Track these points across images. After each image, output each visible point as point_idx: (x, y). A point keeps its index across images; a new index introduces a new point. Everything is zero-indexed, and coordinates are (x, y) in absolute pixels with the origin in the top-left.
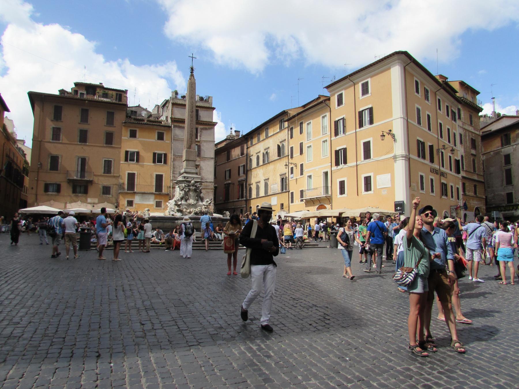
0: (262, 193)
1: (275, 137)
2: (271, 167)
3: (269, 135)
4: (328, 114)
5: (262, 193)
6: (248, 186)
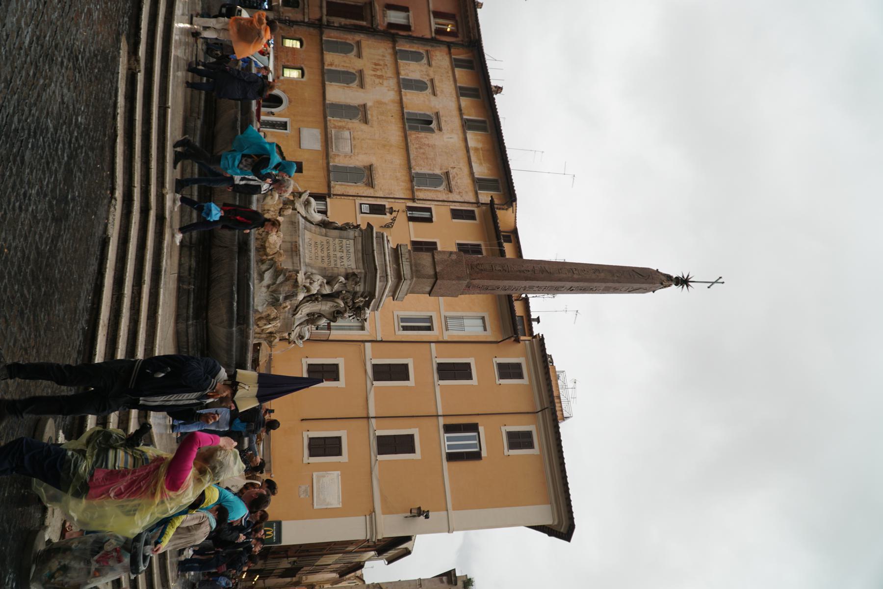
0: (336, 93)
1: (462, 153)
2: (394, 132)
3: (470, 135)
4: (489, 335)
5: (336, 93)
6: (358, 37)
